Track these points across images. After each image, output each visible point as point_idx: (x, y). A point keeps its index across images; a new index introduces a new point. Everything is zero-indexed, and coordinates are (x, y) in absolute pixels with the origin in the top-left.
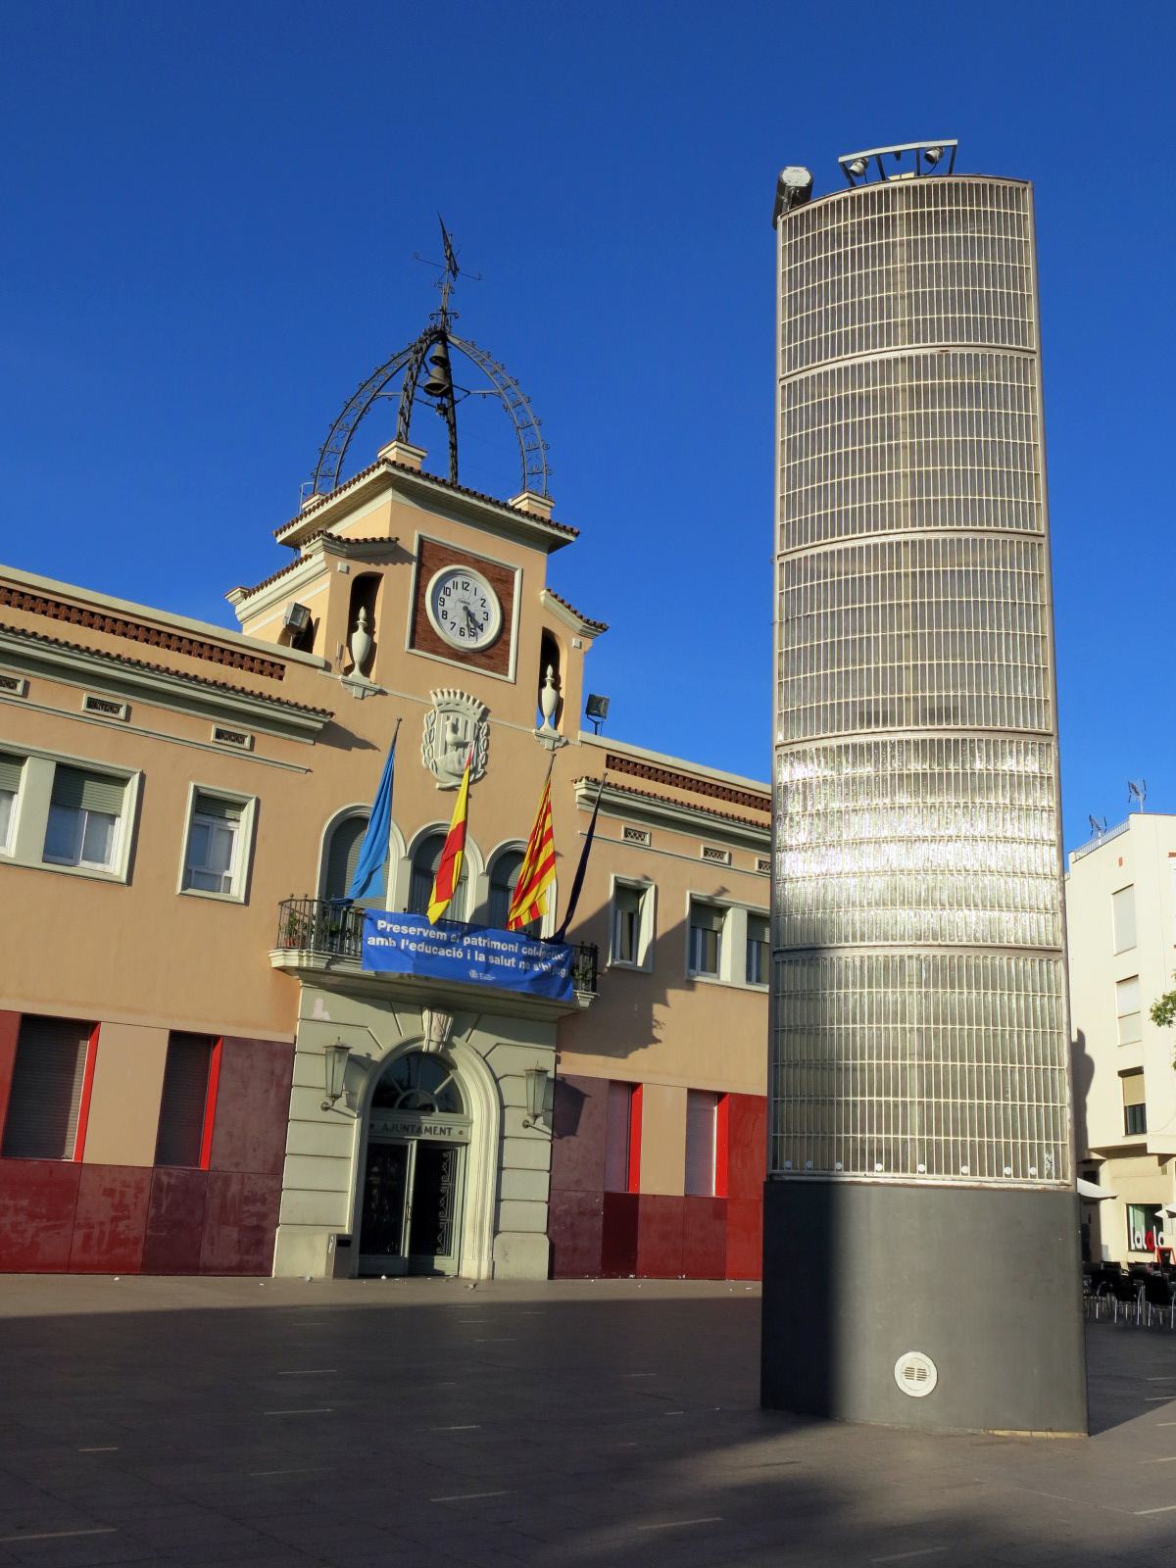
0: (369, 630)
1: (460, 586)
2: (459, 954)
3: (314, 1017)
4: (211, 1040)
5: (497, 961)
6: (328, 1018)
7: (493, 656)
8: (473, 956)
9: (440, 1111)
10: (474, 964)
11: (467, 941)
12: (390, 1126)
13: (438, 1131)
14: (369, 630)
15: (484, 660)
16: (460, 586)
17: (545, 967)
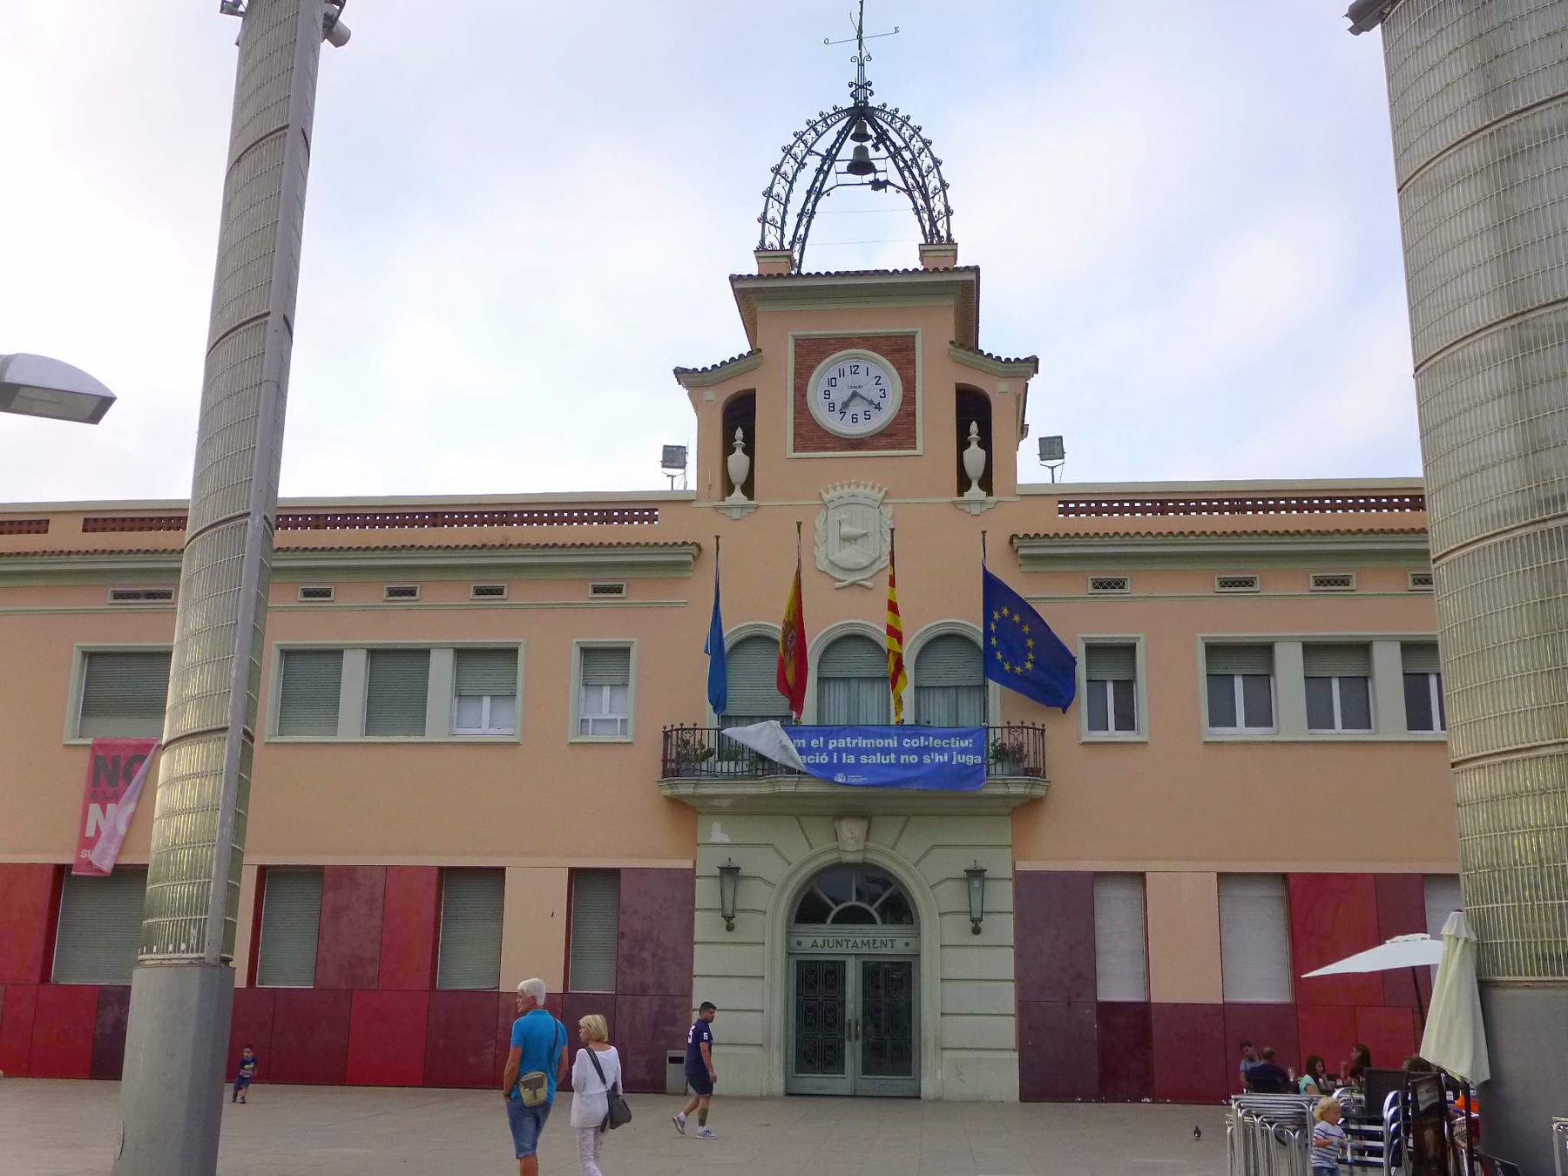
0: (749, 450)
1: (847, 372)
2: (824, 759)
3: (713, 840)
4: (615, 873)
5: (864, 759)
6: (727, 840)
7: (900, 433)
8: (840, 759)
9: (884, 922)
10: (842, 767)
11: (832, 744)
12: (820, 941)
13: (878, 944)
14: (749, 450)
15: (884, 441)
16: (847, 372)
17: (938, 758)
